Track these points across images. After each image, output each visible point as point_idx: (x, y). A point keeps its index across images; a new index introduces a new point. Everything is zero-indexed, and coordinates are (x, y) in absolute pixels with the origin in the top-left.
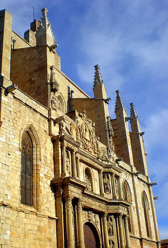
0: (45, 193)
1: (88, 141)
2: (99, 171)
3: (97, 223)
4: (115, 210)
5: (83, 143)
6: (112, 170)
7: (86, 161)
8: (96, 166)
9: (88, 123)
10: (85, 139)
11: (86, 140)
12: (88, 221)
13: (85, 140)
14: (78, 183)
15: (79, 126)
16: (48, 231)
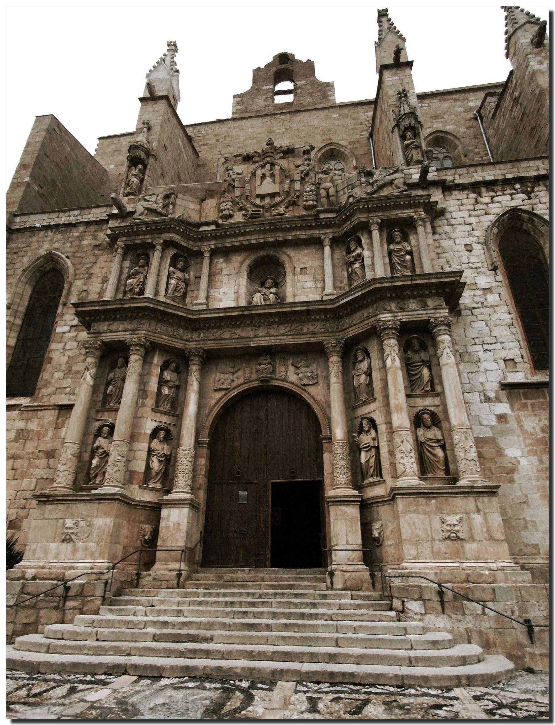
0: (64, 359)
1: (272, 195)
2: (318, 243)
3: (306, 381)
4: (366, 322)
5: (246, 210)
6: (361, 217)
7: (240, 243)
8: (290, 238)
9: (281, 158)
10: (258, 196)
11: (262, 197)
12: (256, 384)
13: (258, 201)
14: (109, 307)
15: (232, 182)
16: (50, 434)
